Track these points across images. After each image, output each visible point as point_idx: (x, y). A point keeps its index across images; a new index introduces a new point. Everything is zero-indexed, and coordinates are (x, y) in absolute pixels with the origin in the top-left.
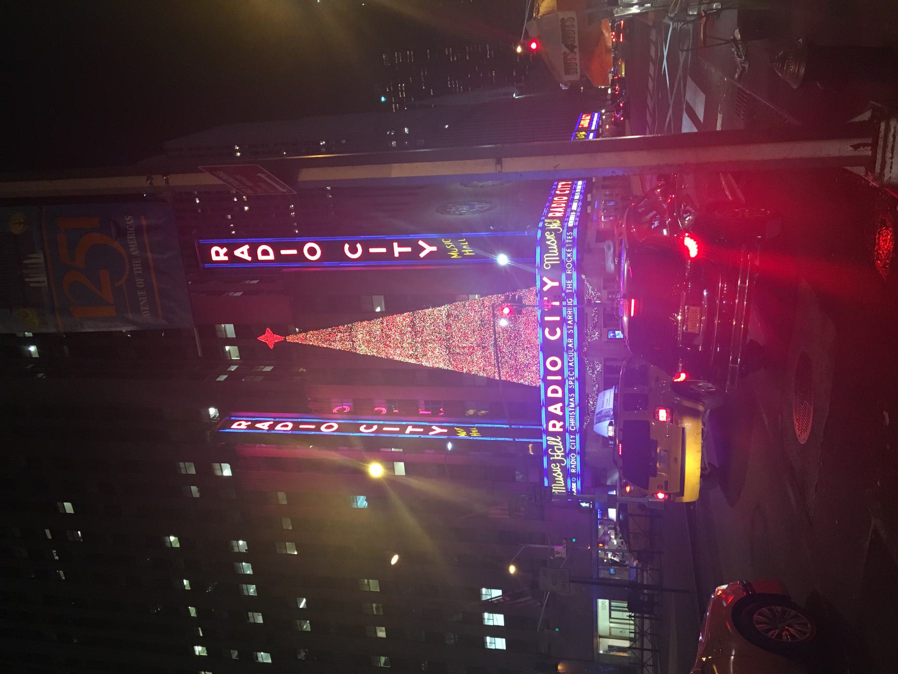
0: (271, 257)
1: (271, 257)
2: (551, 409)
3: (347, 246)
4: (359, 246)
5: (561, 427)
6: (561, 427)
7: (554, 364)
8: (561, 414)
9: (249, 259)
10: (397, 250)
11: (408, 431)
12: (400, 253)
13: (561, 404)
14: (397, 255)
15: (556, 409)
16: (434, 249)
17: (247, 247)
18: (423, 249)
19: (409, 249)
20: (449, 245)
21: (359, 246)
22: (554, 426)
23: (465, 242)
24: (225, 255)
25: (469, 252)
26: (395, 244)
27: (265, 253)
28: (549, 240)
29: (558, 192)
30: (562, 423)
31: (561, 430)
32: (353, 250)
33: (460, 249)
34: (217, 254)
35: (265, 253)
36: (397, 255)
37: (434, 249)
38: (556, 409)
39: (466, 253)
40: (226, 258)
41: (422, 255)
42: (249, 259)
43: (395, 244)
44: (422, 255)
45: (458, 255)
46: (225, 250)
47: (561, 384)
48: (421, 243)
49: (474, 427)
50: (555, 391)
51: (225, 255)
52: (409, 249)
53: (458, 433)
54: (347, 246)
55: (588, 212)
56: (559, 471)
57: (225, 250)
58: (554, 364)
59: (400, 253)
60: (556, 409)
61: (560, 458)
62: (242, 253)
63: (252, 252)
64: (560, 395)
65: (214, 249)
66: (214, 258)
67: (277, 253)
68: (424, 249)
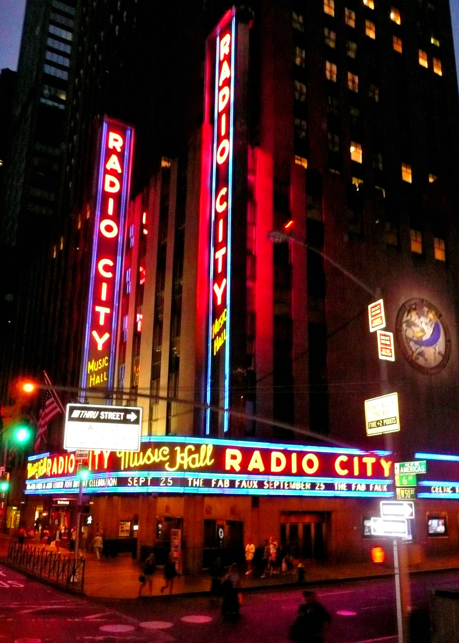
11: (98, 309)
49: (107, 377)
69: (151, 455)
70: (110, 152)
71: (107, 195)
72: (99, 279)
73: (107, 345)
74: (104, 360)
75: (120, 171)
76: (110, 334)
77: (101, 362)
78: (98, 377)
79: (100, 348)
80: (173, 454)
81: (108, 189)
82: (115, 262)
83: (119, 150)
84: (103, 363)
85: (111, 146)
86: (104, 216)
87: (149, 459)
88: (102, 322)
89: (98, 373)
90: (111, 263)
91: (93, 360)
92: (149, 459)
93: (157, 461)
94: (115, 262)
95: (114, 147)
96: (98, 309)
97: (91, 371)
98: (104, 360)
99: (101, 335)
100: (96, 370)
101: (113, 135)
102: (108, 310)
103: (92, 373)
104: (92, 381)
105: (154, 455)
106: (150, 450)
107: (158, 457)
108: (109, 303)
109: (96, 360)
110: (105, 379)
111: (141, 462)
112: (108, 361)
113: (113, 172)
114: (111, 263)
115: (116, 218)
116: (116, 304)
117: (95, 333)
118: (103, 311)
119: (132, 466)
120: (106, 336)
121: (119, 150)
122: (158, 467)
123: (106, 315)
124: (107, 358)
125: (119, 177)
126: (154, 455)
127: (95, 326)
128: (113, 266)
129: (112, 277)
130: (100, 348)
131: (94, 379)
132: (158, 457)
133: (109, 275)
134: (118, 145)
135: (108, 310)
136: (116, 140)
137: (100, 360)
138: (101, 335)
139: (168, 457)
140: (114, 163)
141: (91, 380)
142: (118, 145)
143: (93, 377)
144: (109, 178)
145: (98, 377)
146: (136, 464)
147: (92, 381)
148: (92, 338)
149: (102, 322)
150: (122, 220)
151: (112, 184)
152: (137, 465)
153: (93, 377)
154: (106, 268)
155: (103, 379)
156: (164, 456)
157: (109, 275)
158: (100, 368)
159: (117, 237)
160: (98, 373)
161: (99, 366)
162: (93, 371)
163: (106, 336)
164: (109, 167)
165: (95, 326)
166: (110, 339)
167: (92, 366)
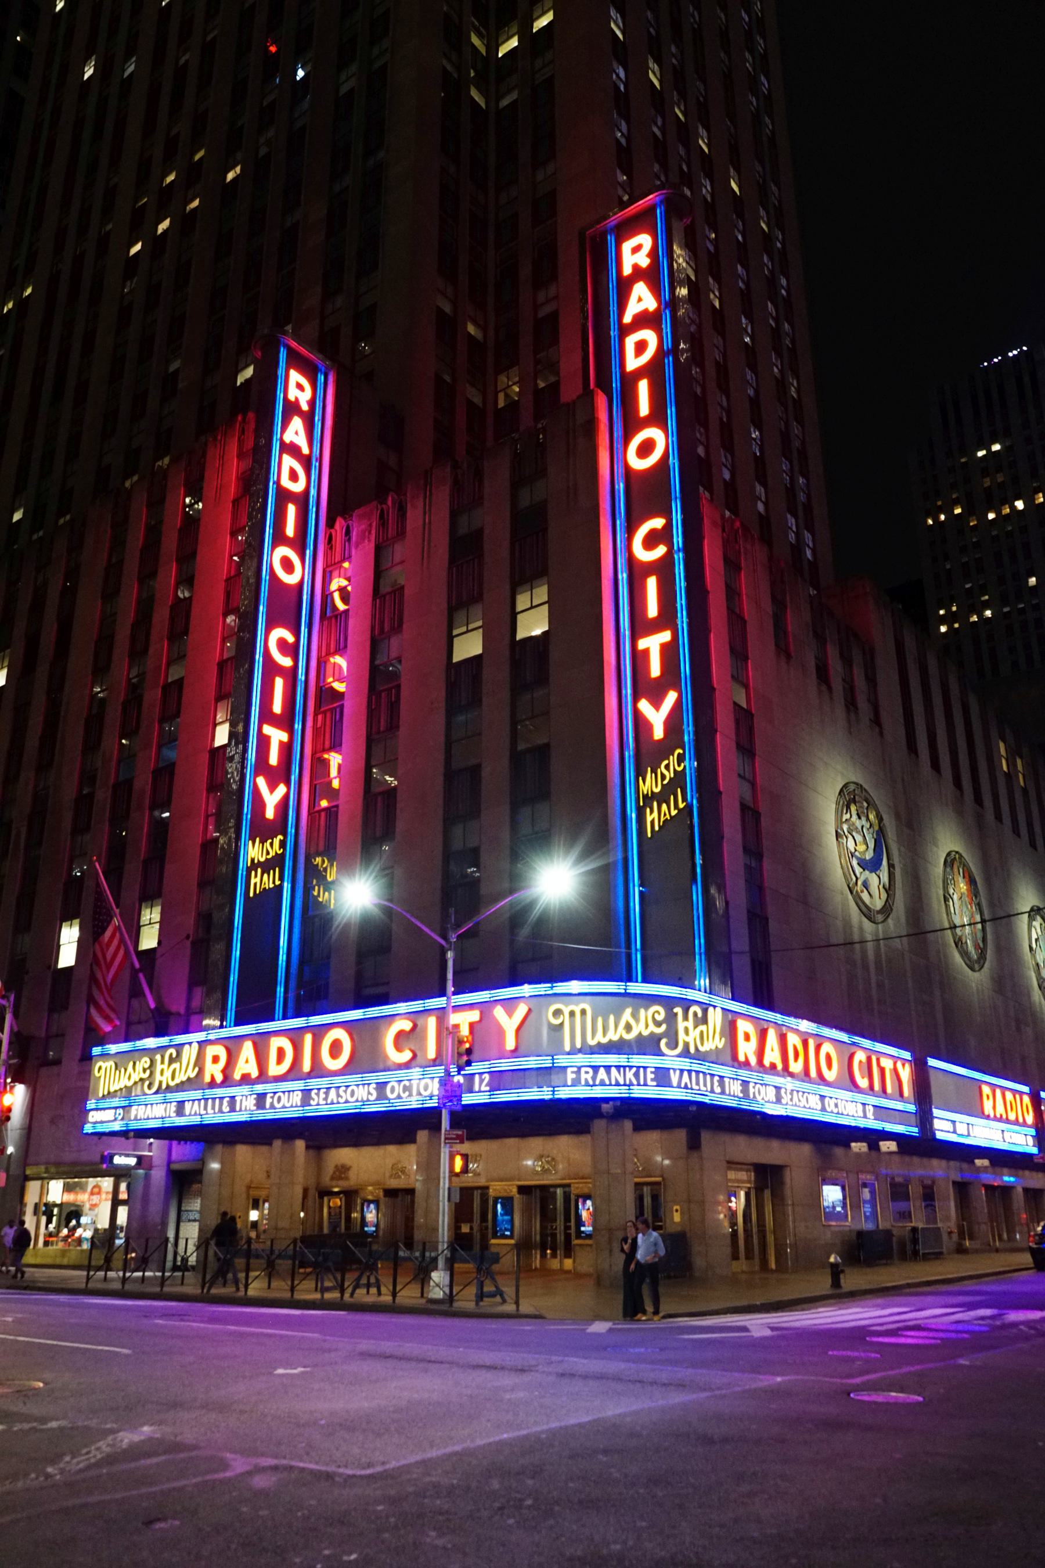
0: (633, 363)
1: (633, 363)
2: (248, 1049)
3: (658, 523)
4: (661, 550)
5: (213, 1077)
6: (213, 1077)
7: (336, 1049)
8: (237, 1076)
9: (627, 319)
10: (653, 643)
11: (267, 729)
12: (646, 652)
13: (255, 1074)
14: (642, 644)
15: (247, 1061)
16: (658, 733)
17: (650, 304)
18: (657, 705)
19: (655, 671)
20: (667, 767)
21: (661, 550)
22: (216, 1059)
23: (676, 806)
24: (636, 267)
25: (652, 822)
26: (666, 636)
27: (641, 347)
28: (635, 1016)
29: (860, 1056)
30: (219, 1078)
31: (207, 1079)
32: (650, 542)
33: (662, 798)
34: (636, 249)
35: (641, 347)
36: (642, 644)
37: (658, 733)
38: (246, 1063)
39: (652, 812)
40: (627, 270)
41: (644, 706)
42: (627, 319)
43: (666, 636)
44: (644, 706)
45: (645, 797)
46: (644, 261)
47: (293, 1073)
48: (672, 697)
49: (281, 878)
50: (281, 1053)
51: (636, 267)
52: (655, 671)
53: (262, 842)
54: (658, 523)
55: (853, 1144)
56: (135, 1077)
57: (644, 261)
58: (336, 1049)
59: (646, 652)
60: (246, 1063)
61: (158, 1077)
62: (640, 300)
63: (643, 320)
64: (275, 1069)
65: (645, 240)
66: (627, 246)
67: (639, 373)
68: (657, 705)
69: (632, 1022)
70: (292, 408)
71: (284, 496)
72: (271, 669)
73: (283, 805)
74: (277, 842)
75: (306, 451)
76: (288, 785)
77: (272, 844)
78: (266, 876)
79: (270, 814)
80: (671, 1018)
81: (286, 482)
82: (297, 634)
83: (305, 407)
84: (274, 847)
85: (291, 397)
86: (280, 538)
87: (628, 1028)
88: (273, 760)
89: (267, 866)
90: (291, 639)
91: (258, 840)
92: (628, 1028)
93: (646, 1033)
94: (297, 634)
95: (297, 399)
96: (267, 729)
97: (253, 860)
98: (277, 842)
99: (272, 788)
100: (262, 860)
101: (295, 376)
102: (284, 737)
103: (254, 866)
104: (255, 884)
105: (637, 1020)
106: (628, 1011)
107: (647, 1026)
108: (285, 722)
109: (262, 842)
110: (278, 883)
111: (613, 1036)
112: (283, 844)
113: (292, 449)
114: (291, 639)
115: (299, 544)
116: (298, 726)
117: (261, 781)
118: (277, 736)
119: (592, 1042)
120: (282, 789)
121: (305, 407)
122: (648, 1045)
123: (281, 743)
124: (280, 837)
125: (306, 462)
126: (637, 1020)
127: (262, 766)
128: (294, 642)
129: (291, 667)
130: (270, 814)
131: (258, 880)
132: (647, 1026)
133: (286, 662)
134: (304, 398)
135: (284, 737)
136: (300, 387)
137: (270, 841)
138: (272, 788)
139: (664, 1027)
140: (296, 433)
141: (253, 881)
142: (304, 398)
143: (256, 876)
144: (288, 461)
145: (266, 876)
146: (601, 1038)
147: (255, 884)
148: (256, 791)
149: (273, 760)
150: (308, 553)
151: (294, 476)
152: (604, 1041)
153: (256, 876)
154: (282, 644)
155: (274, 882)
156: (658, 1024)
157: (286, 662)
158: (269, 857)
159: (301, 583)
160: (267, 866)
161: (268, 853)
162: (256, 861)
163: (282, 789)
164: (288, 438)
165: (262, 766)
166: (286, 797)
167: (254, 852)
